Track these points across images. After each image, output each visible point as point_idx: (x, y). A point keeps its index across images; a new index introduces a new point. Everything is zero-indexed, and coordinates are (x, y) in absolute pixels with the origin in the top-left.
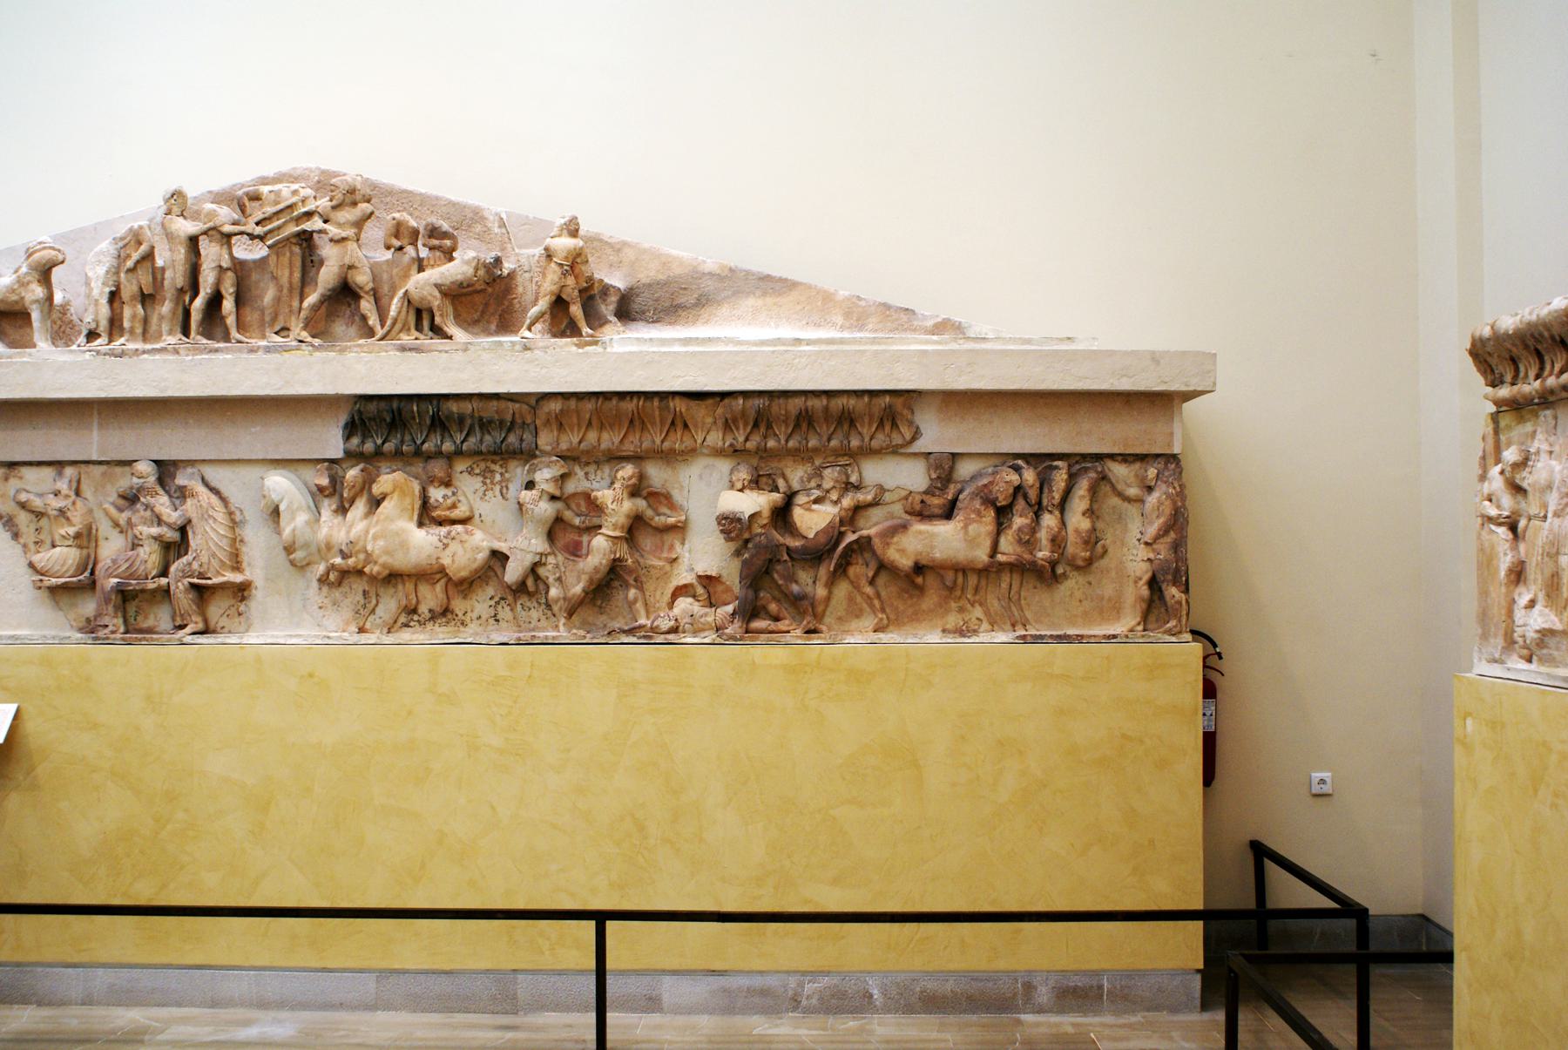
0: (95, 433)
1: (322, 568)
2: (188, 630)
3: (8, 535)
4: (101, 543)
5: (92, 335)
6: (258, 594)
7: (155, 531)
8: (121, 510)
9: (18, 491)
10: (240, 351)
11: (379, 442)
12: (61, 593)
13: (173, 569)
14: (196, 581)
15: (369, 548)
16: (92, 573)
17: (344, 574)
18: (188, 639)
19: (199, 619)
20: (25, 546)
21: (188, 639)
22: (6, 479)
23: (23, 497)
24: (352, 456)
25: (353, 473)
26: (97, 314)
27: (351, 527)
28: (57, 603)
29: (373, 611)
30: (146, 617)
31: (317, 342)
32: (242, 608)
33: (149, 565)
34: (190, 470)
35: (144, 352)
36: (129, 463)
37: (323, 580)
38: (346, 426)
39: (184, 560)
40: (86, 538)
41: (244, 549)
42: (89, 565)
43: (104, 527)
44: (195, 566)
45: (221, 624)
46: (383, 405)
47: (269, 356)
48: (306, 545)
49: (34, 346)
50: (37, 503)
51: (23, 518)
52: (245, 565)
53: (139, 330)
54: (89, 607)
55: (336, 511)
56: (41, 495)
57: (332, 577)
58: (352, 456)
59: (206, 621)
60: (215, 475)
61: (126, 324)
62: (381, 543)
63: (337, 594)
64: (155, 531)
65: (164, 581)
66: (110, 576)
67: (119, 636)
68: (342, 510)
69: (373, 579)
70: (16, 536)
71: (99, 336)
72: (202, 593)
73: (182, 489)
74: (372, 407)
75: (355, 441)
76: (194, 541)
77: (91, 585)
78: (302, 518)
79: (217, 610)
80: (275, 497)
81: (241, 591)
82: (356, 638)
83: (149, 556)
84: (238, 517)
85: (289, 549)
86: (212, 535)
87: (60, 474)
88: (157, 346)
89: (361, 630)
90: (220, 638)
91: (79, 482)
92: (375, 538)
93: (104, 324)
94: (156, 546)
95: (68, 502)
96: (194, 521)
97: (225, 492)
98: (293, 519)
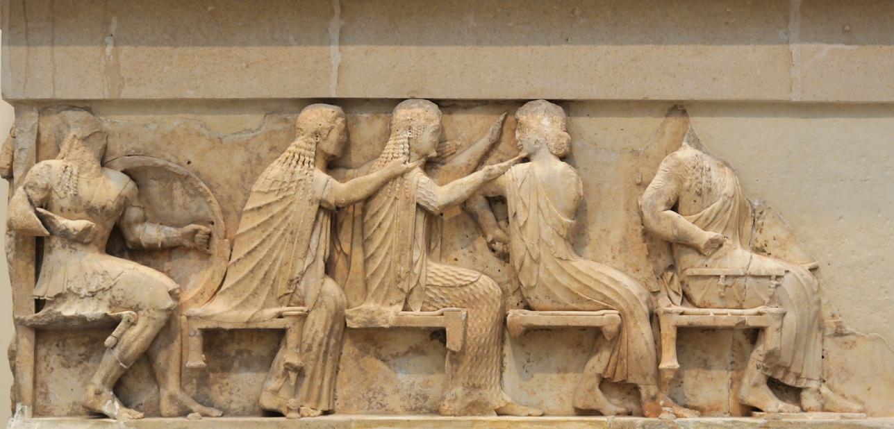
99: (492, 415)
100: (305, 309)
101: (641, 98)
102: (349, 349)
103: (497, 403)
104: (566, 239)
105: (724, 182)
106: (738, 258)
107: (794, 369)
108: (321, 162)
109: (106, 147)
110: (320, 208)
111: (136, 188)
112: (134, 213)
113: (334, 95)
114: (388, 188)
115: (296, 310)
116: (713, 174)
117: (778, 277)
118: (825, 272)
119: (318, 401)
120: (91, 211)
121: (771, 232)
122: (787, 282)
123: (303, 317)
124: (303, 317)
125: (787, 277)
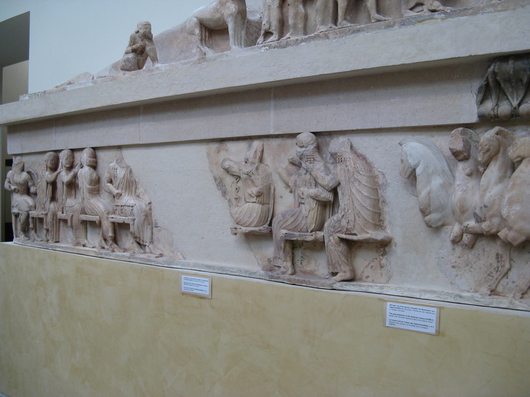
0: (272, 112)
1: (456, 229)
2: (338, 277)
3: (219, 193)
4: (278, 200)
5: (268, 34)
6: (398, 250)
7: (313, 191)
8: (290, 174)
9: (224, 160)
10: (379, 28)
11: (515, 103)
12: (252, 238)
13: (326, 225)
14: (344, 236)
15: (504, 212)
16: (270, 225)
17: (478, 236)
18: (338, 286)
19: (347, 269)
20: (230, 201)
21: (338, 286)
22: (219, 152)
23: (227, 164)
24: (486, 121)
25: (487, 136)
26: (269, 18)
27: (485, 190)
28: (249, 245)
29: (506, 274)
30: (309, 262)
31: (448, 9)
32: (384, 261)
33: (309, 220)
34: (342, 139)
35: (302, 41)
36: (293, 136)
37: (456, 241)
38: (479, 91)
39: (335, 217)
40: (265, 196)
41: (386, 209)
42: (269, 219)
43: (280, 188)
44: (344, 223)
45: (366, 274)
46: (520, 64)
47: (404, 29)
48: (441, 208)
49: (229, 49)
50: (235, 169)
51: (229, 180)
52: (386, 223)
53: (301, 26)
54: (269, 250)
55: (470, 175)
56: (237, 163)
57: (466, 238)
58: (486, 121)
59: (353, 271)
60: (363, 143)
61: (291, 21)
62: (517, 208)
63: (470, 255)
64: (313, 191)
65: (320, 234)
66: (281, 228)
67: (287, 276)
68: (476, 173)
69: (508, 245)
70: (224, 193)
71: (271, 34)
72: (351, 246)
73: (334, 155)
74: (510, 66)
75: (489, 106)
76: (343, 201)
77: (268, 235)
78: (437, 182)
79: (363, 261)
80: (412, 162)
81: (383, 246)
82: (488, 300)
83: (309, 212)
84: (381, 181)
85: (424, 212)
86: (358, 196)
87: (250, 146)
88: (313, 35)
89: (493, 292)
90: (364, 286)
91: (262, 151)
92: (511, 203)
93: (275, 23)
94: (313, 204)
95: (253, 168)
96: (343, 183)
97: (370, 159)
98: (429, 182)
99: (81, 246)
100: (46, 212)
101: (107, 145)
102: (62, 224)
103: (83, 243)
104: (89, 193)
105: (121, 173)
106: (127, 200)
107: (142, 238)
108: (48, 169)
109: (24, 166)
110: (48, 183)
111: (30, 177)
112: (30, 184)
113: (54, 149)
114: (58, 177)
115: (44, 212)
116: (118, 171)
117: (132, 206)
118: (153, 205)
119: (53, 239)
120: (17, 184)
121: (140, 190)
122: (135, 208)
123: (46, 215)
124: (46, 215)
125: (135, 207)
